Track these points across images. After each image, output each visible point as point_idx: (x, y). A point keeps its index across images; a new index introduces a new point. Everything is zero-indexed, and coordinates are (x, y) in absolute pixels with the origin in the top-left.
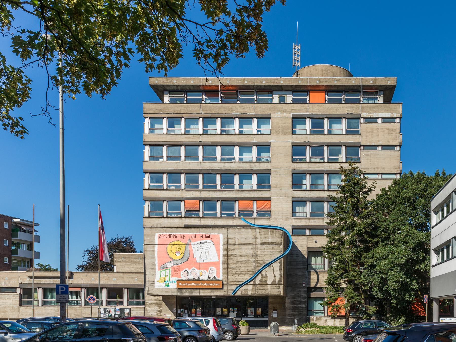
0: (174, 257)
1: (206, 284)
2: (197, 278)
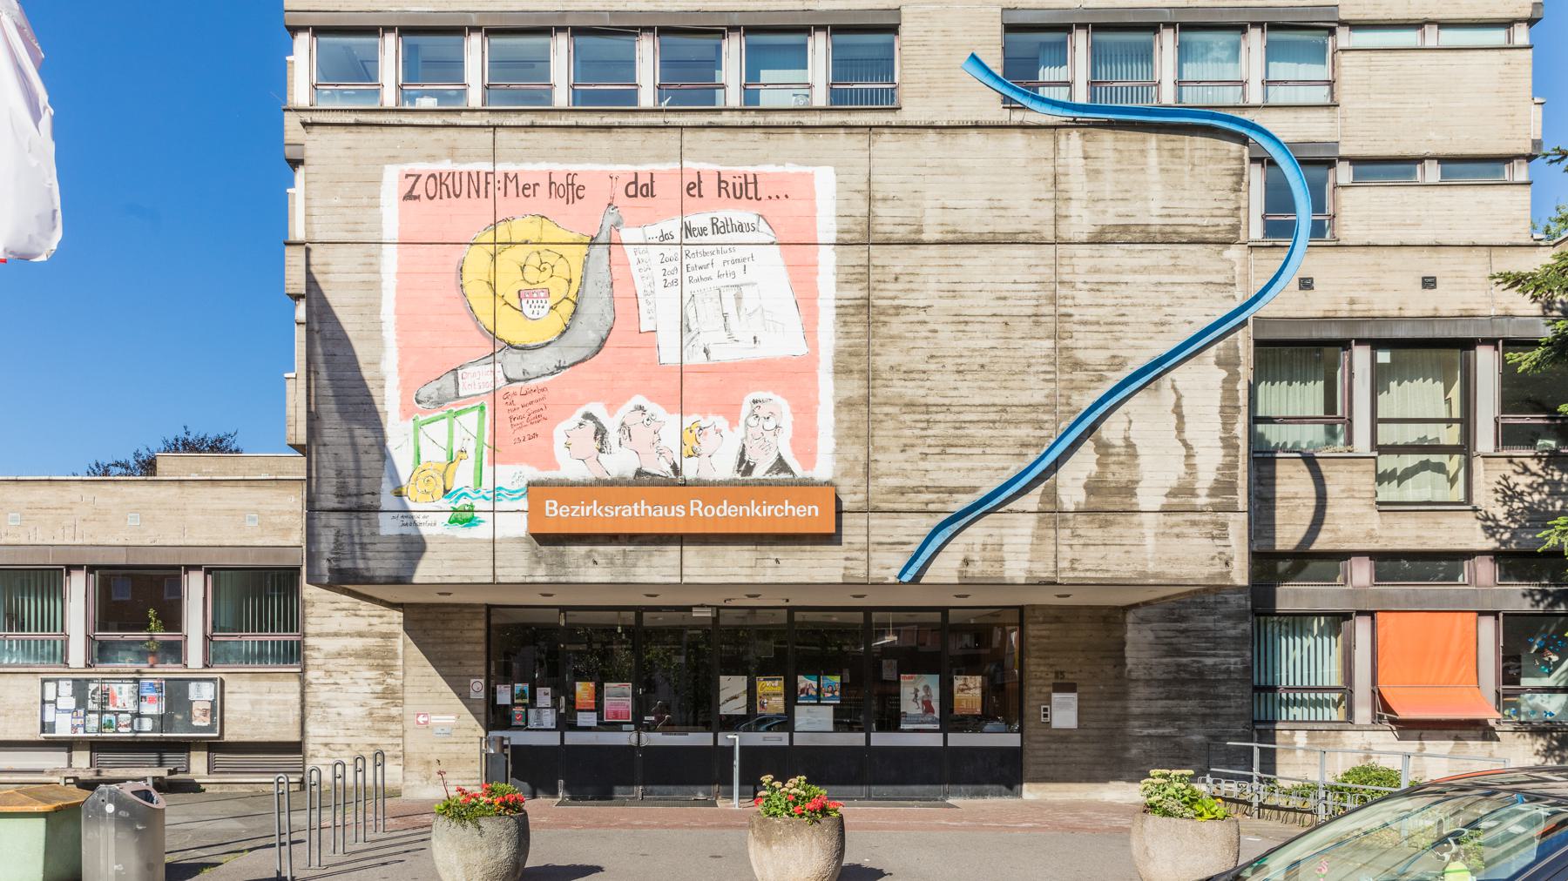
0: (511, 329)
2: (662, 468)
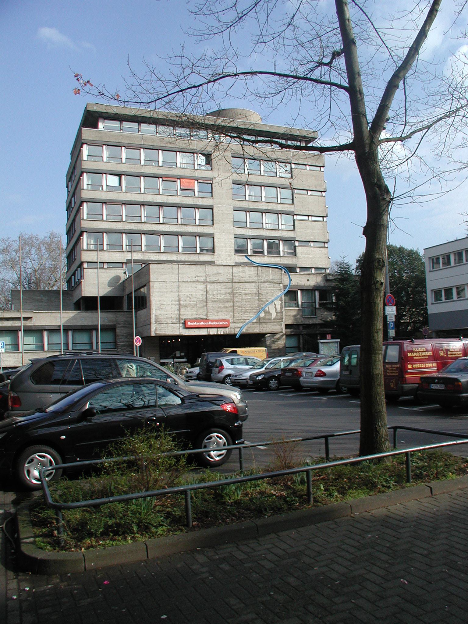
1: (214, 323)
